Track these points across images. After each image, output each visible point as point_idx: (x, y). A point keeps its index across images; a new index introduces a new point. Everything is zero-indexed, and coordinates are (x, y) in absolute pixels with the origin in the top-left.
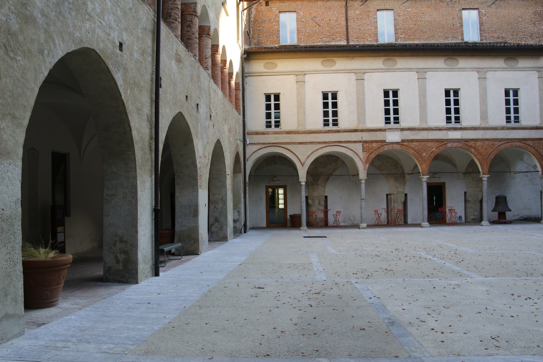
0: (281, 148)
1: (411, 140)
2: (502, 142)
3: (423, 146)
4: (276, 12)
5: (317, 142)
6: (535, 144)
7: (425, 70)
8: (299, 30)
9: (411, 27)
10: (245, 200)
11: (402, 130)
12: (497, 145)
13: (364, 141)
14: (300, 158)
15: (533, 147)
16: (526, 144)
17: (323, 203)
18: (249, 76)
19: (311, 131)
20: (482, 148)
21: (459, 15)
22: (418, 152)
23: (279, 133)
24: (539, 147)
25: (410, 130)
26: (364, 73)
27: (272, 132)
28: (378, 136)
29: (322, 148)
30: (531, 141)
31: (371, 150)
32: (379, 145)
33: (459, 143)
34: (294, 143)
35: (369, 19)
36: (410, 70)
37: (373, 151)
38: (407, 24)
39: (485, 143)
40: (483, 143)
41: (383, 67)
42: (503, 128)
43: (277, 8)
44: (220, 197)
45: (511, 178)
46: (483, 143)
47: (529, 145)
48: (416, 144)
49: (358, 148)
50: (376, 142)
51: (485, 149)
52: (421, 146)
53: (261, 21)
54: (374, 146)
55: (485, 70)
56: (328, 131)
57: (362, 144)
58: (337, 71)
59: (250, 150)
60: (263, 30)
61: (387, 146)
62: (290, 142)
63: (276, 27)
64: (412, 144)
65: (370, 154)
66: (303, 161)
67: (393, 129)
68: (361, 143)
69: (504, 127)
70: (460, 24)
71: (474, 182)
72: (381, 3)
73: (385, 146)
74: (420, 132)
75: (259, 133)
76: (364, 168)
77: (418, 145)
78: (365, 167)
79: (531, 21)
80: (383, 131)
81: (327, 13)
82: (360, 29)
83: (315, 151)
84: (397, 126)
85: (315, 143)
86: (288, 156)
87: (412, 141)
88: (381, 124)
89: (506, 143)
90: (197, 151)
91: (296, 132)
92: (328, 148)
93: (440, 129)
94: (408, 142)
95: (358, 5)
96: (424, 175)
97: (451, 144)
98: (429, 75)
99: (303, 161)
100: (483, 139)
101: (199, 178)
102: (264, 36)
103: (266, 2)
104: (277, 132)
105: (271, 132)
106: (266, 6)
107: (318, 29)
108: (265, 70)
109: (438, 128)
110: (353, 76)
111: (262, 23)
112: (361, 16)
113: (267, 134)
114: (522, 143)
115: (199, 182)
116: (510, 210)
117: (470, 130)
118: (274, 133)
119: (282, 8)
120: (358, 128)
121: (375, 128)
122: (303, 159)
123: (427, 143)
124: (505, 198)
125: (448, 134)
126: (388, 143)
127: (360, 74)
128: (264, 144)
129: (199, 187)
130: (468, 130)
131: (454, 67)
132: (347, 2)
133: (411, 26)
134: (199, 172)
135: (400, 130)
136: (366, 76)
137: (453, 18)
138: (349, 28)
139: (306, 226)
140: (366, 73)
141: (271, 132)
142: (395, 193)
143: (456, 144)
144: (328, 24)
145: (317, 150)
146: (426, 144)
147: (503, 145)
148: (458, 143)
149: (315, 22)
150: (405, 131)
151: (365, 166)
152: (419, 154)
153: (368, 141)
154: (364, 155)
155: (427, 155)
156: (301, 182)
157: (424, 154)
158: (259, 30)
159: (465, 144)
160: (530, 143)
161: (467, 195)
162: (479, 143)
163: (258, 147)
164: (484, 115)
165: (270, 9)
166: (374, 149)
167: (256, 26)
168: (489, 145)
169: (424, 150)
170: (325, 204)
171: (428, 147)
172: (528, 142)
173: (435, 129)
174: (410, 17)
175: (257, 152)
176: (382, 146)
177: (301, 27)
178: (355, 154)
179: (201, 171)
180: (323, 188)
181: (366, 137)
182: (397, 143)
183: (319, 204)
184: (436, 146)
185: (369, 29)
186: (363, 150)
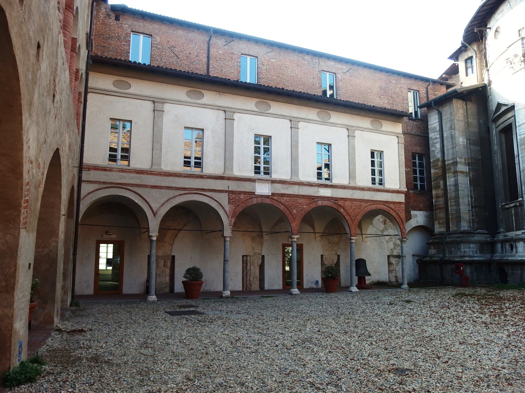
0: (127, 191)
1: (282, 194)
2: (369, 204)
3: (294, 202)
4: (127, 30)
5: (175, 188)
6: (396, 207)
7: (299, 120)
8: (154, 58)
9: (274, 79)
10: (74, 257)
11: (273, 182)
12: (364, 206)
13: (232, 191)
14: (152, 205)
15: (394, 211)
16: (389, 207)
17: (169, 264)
18: (91, 92)
19: (168, 173)
20: (351, 208)
21: (319, 76)
22: (288, 208)
23: (126, 172)
24: (399, 211)
25: (281, 183)
26: (234, 112)
27: (118, 169)
28: (246, 187)
29: (181, 195)
30: (393, 205)
31: (238, 202)
32: (247, 197)
33: (330, 201)
34: (145, 186)
35: (232, 62)
36: (284, 117)
37: (241, 204)
38: (270, 75)
39: (353, 203)
40: (351, 203)
41: (255, 109)
42: (369, 189)
43: (129, 25)
44: (46, 252)
46: (351, 203)
47: (391, 208)
48: (287, 199)
49: (224, 199)
50: (245, 193)
51: (353, 210)
52: (292, 201)
53: (108, 36)
54: (242, 198)
55: (354, 128)
56: (190, 175)
57: (228, 195)
58: (205, 106)
59: (86, 188)
60: (109, 47)
61: (255, 199)
62: (140, 183)
63: (126, 47)
64: (282, 199)
65: (237, 207)
66: (155, 210)
67: (264, 180)
68: (227, 194)
69: (370, 188)
70: (319, 84)
71: (330, 245)
72: (246, 48)
73: (253, 199)
74: (292, 186)
75: (99, 168)
76: (229, 224)
77: (288, 200)
78: (231, 222)
79: (378, 94)
80: (252, 182)
81: (188, 45)
82: (222, 70)
83: (172, 198)
84: (267, 177)
85: (172, 189)
86: (136, 202)
87: (283, 195)
88: (251, 174)
89: (372, 204)
90: (27, 143)
91: (150, 172)
92: (187, 195)
93: (310, 185)
94: (278, 196)
95: (222, 44)
96: (294, 235)
97: (321, 202)
98: (301, 125)
99: (155, 210)
100: (352, 199)
101: (24, 205)
102: (110, 55)
103: (116, 15)
104: (124, 170)
105: (116, 169)
106: (116, 20)
107: (176, 61)
108: (114, 89)
109: (309, 184)
110: (222, 114)
111: (109, 39)
112: (224, 57)
113: (110, 171)
114: (385, 205)
115: (24, 214)
116: (370, 275)
117: (340, 188)
118: (120, 171)
119: (135, 28)
120: (225, 175)
121: (244, 177)
122: (155, 206)
123: (298, 199)
124: (364, 261)
125: (319, 191)
126: (257, 196)
127: (231, 113)
128: (104, 183)
129: (21, 224)
130: (338, 188)
131: (326, 121)
132: (211, 37)
133: (274, 78)
134: (26, 193)
135: (271, 182)
136: (236, 116)
137: (313, 78)
138: (211, 67)
139: (154, 294)
140: (236, 113)
141: (116, 169)
142: (251, 254)
143: (326, 202)
144: (187, 57)
145: (174, 197)
146: (296, 200)
147: (369, 207)
148: (328, 201)
149: (173, 53)
150: (276, 183)
151: (231, 221)
152: (289, 211)
153: (236, 191)
154: (229, 208)
155: (297, 213)
156: (151, 236)
157: (295, 211)
158: (104, 47)
159: (334, 203)
160: (392, 206)
161: (324, 258)
163: (96, 186)
164: (352, 175)
165: (120, 25)
166: (242, 201)
167: (101, 41)
168: (357, 205)
169: (294, 207)
170: (171, 266)
171: (299, 204)
172: (390, 205)
174: (274, 69)
175: (94, 193)
176: (251, 198)
177: (157, 54)
178: (219, 205)
179: (29, 192)
180: (170, 246)
181: (233, 186)
182: (267, 197)
183: (164, 266)
184: (306, 203)
185: (231, 72)
186: (229, 202)
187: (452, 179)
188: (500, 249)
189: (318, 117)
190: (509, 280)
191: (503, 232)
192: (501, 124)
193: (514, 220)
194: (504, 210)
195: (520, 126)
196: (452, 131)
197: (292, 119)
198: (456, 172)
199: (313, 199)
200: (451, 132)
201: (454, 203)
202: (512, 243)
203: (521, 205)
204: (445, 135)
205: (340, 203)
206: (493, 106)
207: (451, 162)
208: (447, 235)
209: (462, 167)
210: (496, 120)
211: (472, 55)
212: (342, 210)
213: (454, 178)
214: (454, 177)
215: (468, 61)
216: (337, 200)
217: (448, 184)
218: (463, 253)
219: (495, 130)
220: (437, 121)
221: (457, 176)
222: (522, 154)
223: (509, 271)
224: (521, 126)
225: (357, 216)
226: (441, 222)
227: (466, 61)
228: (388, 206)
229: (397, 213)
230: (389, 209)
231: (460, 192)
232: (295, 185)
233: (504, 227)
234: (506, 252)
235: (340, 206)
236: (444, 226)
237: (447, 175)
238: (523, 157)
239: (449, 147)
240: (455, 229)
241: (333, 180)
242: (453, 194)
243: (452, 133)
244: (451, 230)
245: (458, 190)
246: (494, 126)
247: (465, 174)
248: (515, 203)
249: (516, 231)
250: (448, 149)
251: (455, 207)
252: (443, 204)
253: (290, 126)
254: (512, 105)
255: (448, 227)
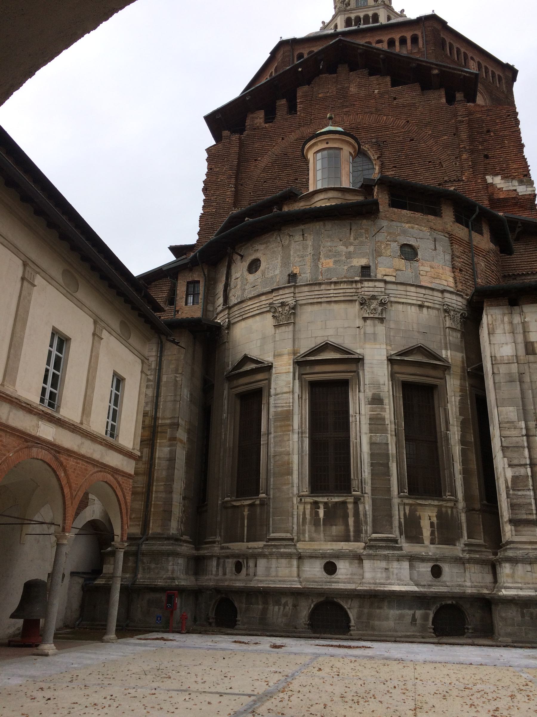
7: (38, 270)
36: (16, 250)
45: (20, 543)
47: (118, 482)
51: (76, 477)
69: (104, 440)
109: (29, 407)
125: (38, 426)
143: (44, 451)
162: (71, 463)
168: (81, 468)
173: (24, 405)
184: (15, 447)
187: (166, 450)
188: (215, 569)
189: (63, 279)
190: (239, 620)
191: (218, 541)
192: (243, 385)
193: (246, 525)
194: (226, 508)
195: (276, 395)
196: (177, 375)
197: (30, 263)
198: (173, 439)
199: (26, 441)
200: (176, 377)
201: (162, 487)
202: (241, 560)
203: (264, 504)
204: (164, 378)
205: (62, 459)
206: (230, 357)
207: (168, 421)
208: (144, 541)
209: (182, 434)
210: (231, 378)
211: (199, 280)
212: (63, 475)
213: (169, 449)
214: (170, 446)
215: (190, 285)
216: (59, 453)
217: (157, 456)
218: (170, 573)
219: (229, 393)
220: (154, 354)
221: (175, 445)
222: (275, 432)
223: (240, 605)
224: (279, 396)
225: (78, 491)
226: (133, 516)
227: (188, 283)
228: (116, 479)
229: (124, 494)
230: (117, 485)
231: (176, 471)
232: (5, 401)
233: (222, 534)
234: (225, 574)
235: (61, 464)
236: (139, 525)
237: (158, 441)
238: (277, 437)
239: (169, 398)
240: (159, 530)
241: (61, 410)
242: (164, 473)
243: (178, 379)
244: (150, 532)
245: (174, 468)
246: (226, 386)
247: (183, 445)
248: (252, 501)
249: (247, 541)
250: (165, 402)
251: (163, 495)
252: (143, 487)
253: (20, 274)
254: (270, 364)
255: (145, 526)
